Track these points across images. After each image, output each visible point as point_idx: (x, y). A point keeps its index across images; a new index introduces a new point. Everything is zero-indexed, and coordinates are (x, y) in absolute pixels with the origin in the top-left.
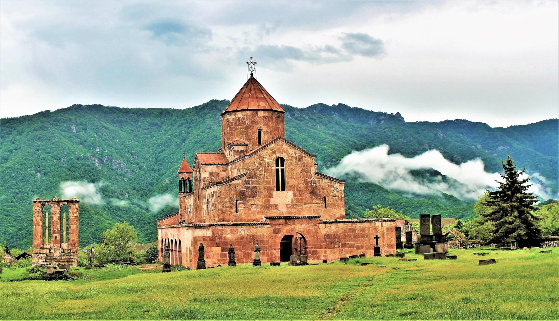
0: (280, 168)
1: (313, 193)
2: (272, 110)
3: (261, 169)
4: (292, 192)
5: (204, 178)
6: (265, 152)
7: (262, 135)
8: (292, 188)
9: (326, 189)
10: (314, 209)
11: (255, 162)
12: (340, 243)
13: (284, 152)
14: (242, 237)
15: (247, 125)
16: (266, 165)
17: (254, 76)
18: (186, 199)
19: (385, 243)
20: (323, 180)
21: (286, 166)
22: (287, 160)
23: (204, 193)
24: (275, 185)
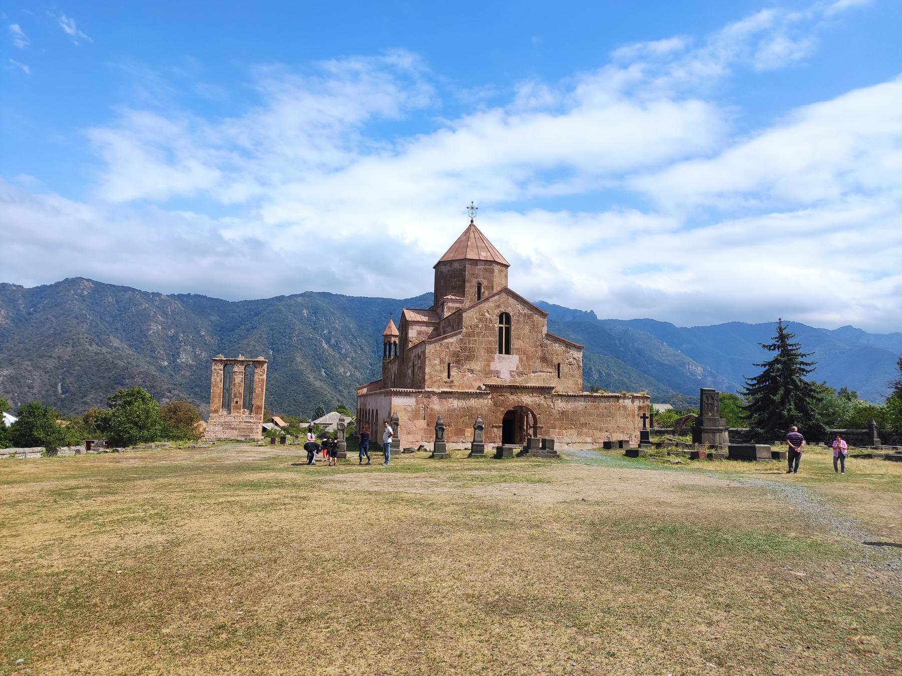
1: (544, 359)
2: (495, 262)
3: (480, 326)
7: (483, 290)
8: (519, 351)
9: (561, 354)
10: (544, 379)
14: (455, 409)
16: (487, 321)
17: (474, 223)
18: (391, 365)
19: (636, 426)
21: (512, 323)
22: (513, 316)
23: (410, 355)
24: (498, 347)
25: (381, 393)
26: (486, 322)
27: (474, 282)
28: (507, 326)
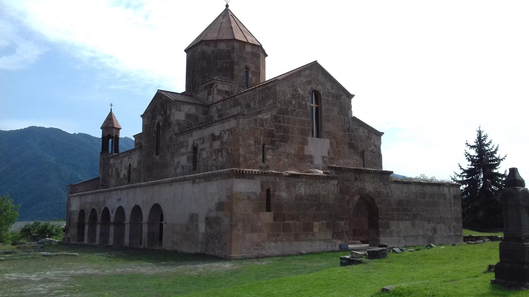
0: (314, 105)
1: (351, 146)
3: (294, 103)
4: (329, 140)
5: (178, 121)
6: (299, 80)
7: (250, 76)
8: (330, 135)
11: (288, 92)
12: (411, 213)
13: (321, 85)
15: (233, 59)
16: (299, 98)
17: (229, 8)
20: (361, 130)
21: (323, 103)
25: (185, 180)
26: (300, 100)
27: (242, 67)
28: (316, 106)
